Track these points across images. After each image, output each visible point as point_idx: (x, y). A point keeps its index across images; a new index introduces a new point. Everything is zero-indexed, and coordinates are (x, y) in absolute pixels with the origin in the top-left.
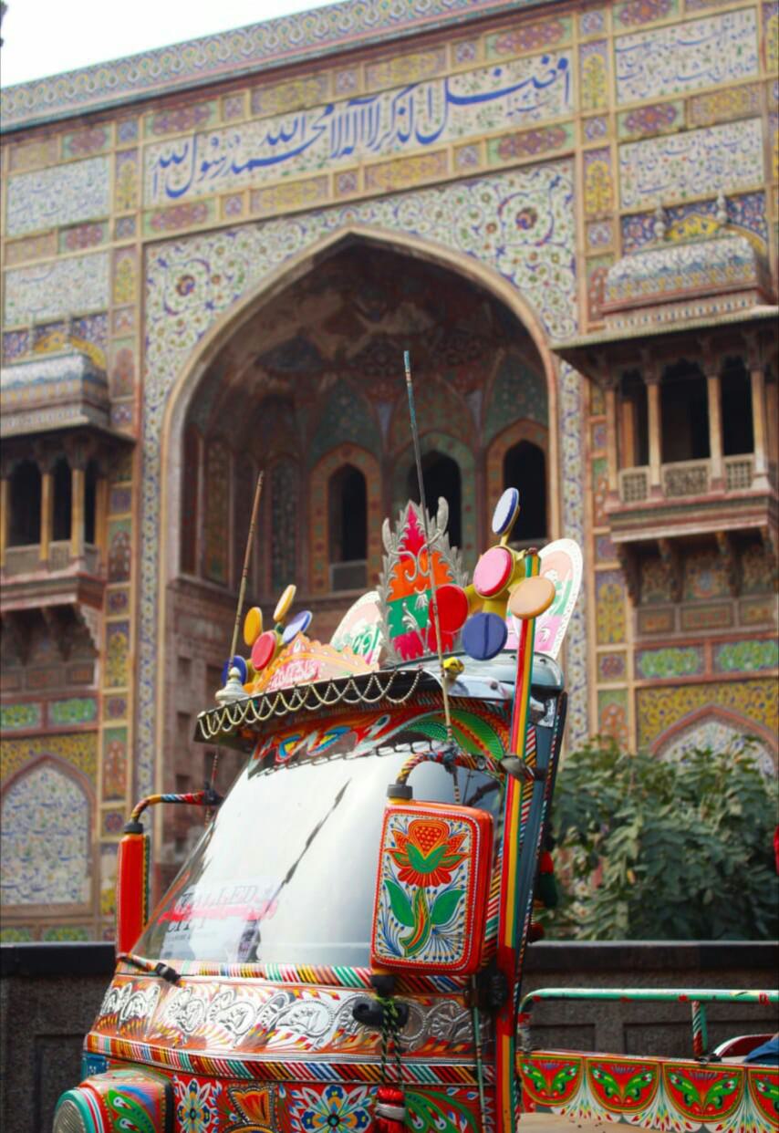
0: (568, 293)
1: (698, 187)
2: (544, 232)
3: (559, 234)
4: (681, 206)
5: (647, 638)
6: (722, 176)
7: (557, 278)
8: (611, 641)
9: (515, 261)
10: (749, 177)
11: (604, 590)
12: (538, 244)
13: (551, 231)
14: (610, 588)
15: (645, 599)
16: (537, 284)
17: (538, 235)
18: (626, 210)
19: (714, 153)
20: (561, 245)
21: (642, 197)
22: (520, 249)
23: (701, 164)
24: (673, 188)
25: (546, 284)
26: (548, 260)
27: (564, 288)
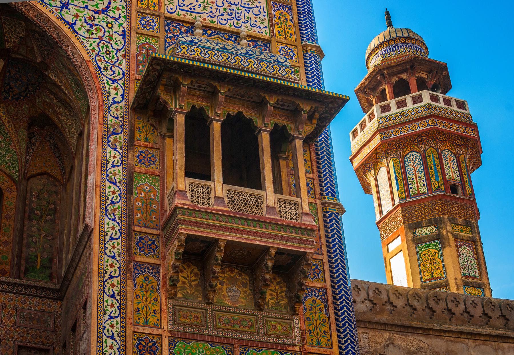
0: (119, 50)
1: (223, 22)
2: (101, 7)
3: (114, 12)
4: (210, 28)
5: (181, 329)
6: (240, 22)
7: (110, 37)
8: (146, 324)
9: (77, 16)
10: (259, 29)
11: (140, 278)
12: (96, 12)
13: (108, 7)
14: (146, 278)
15: (179, 295)
16: (94, 36)
17: (97, 6)
18: (167, 14)
19: (233, 7)
20: (116, 19)
21: (181, 12)
22: (82, 10)
23: (225, 9)
24: (205, 16)
25: (101, 38)
26: (104, 24)
27: (115, 46)
